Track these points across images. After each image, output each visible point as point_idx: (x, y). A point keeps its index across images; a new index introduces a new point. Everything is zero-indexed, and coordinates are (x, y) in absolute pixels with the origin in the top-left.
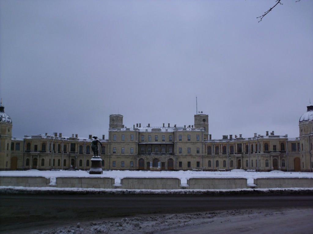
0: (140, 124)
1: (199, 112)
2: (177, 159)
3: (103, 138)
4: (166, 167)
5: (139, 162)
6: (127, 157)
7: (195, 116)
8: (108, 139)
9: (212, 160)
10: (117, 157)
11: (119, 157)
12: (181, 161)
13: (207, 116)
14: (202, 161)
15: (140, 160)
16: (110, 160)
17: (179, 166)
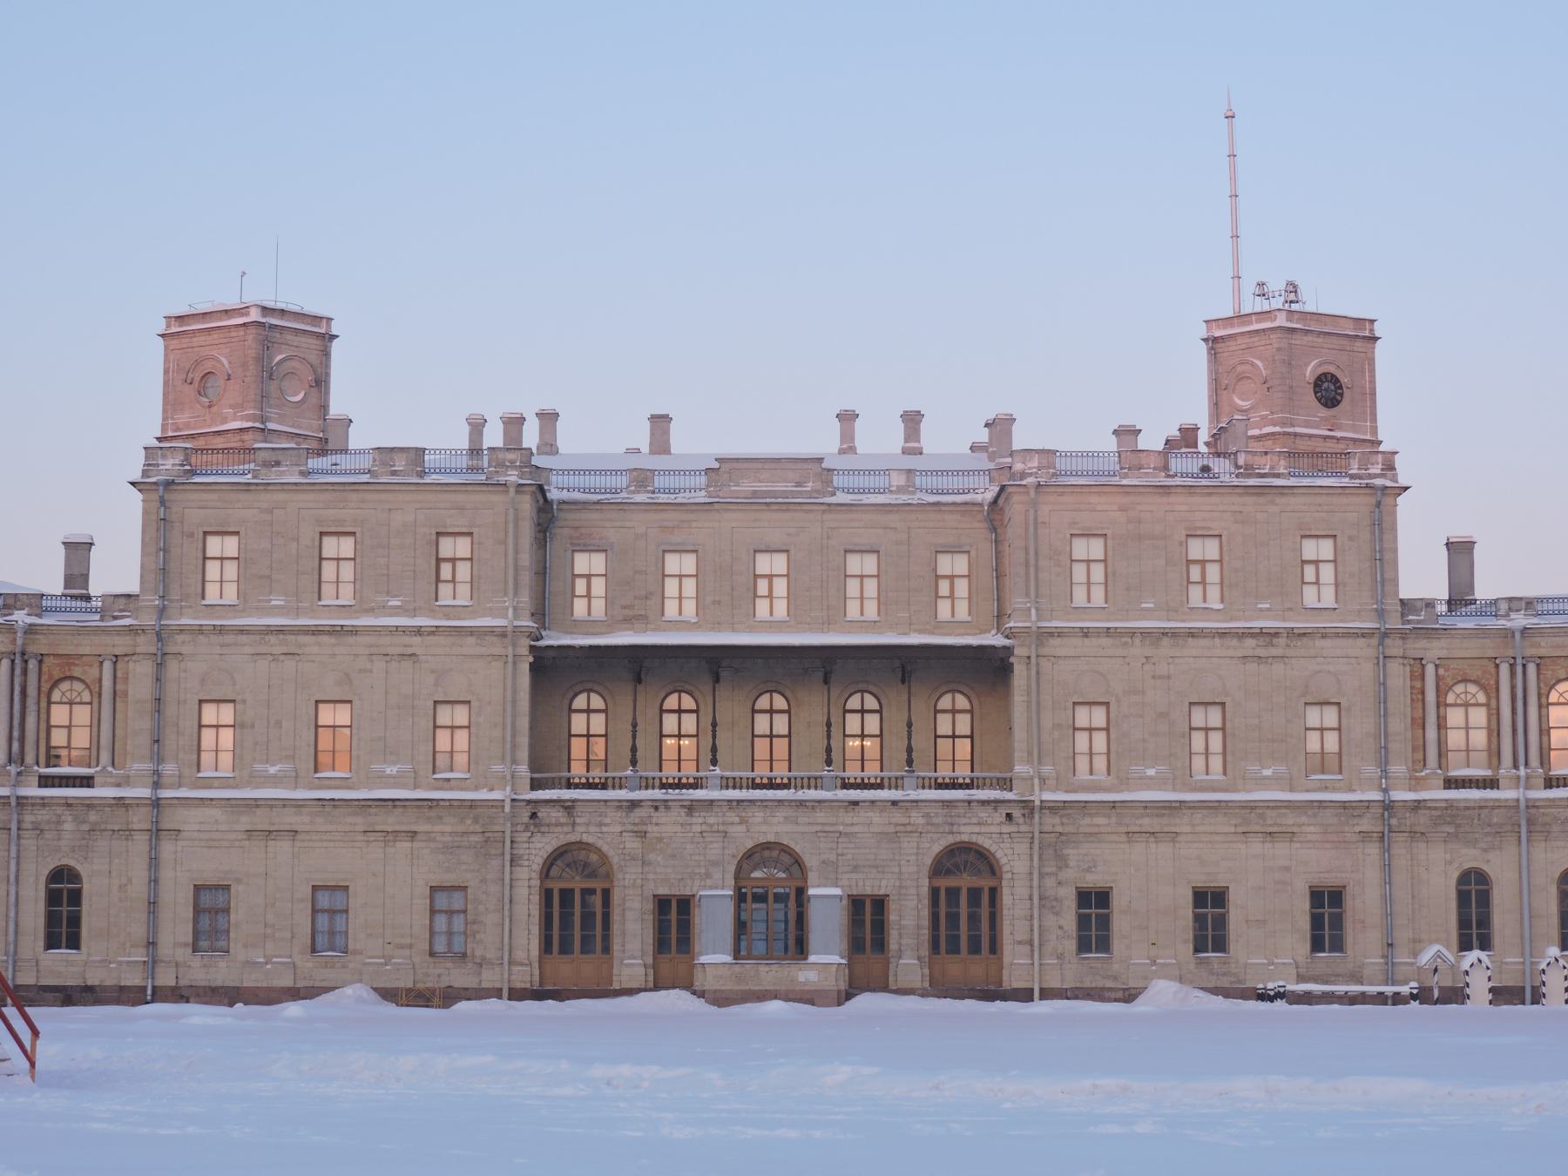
0: (548, 419)
1: (1262, 291)
2: (1052, 849)
3: (76, 578)
4: (908, 960)
5: (547, 895)
6: (391, 821)
7: (1213, 342)
8: (133, 587)
9: (1501, 868)
10: (245, 822)
11: (290, 819)
12: (1093, 880)
13: (1362, 335)
14: (1372, 875)
15: (546, 872)
16: (154, 862)
17: (1071, 945)
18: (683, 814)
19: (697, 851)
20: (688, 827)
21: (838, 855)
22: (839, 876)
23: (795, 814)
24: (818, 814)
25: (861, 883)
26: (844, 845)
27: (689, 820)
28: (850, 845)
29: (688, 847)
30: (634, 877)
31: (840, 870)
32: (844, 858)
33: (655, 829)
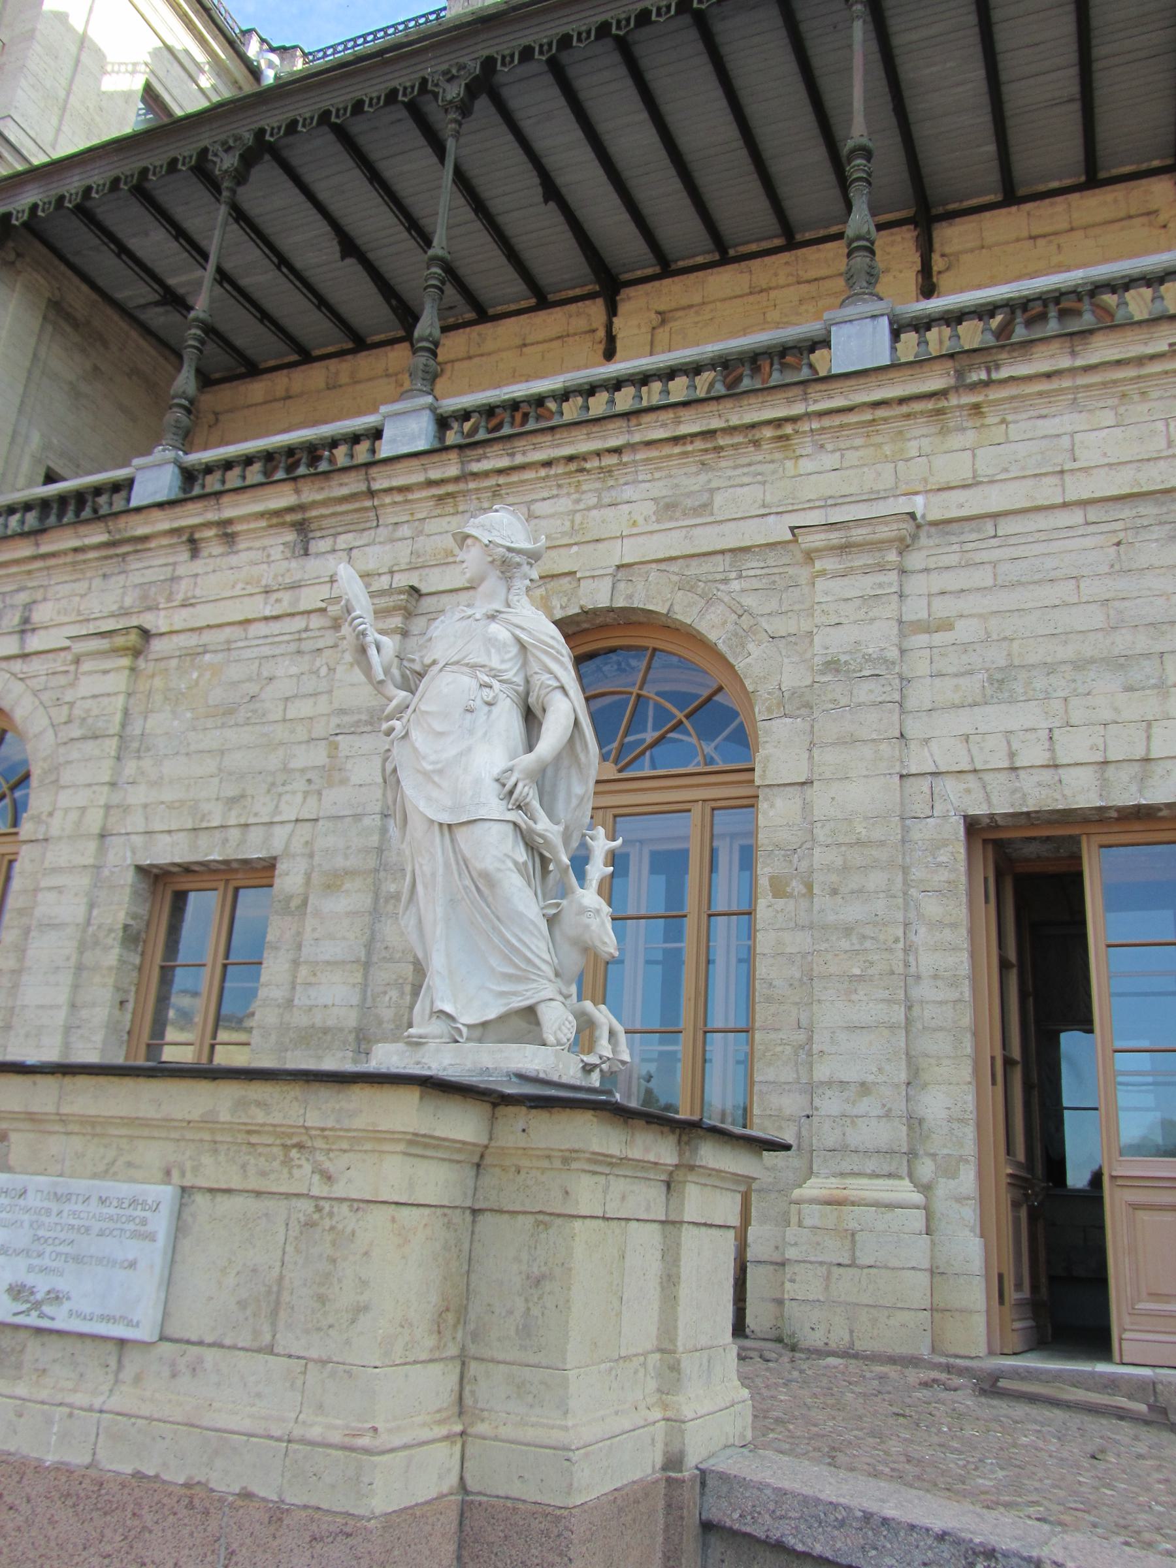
18: (277, 553)
19: (309, 684)
20: (286, 596)
21: (905, 627)
22: (914, 729)
23: (703, 478)
24: (806, 465)
25: (1033, 754)
26: (937, 582)
27: (297, 569)
28: (951, 581)
29: (280, 672)
30: (81, 798)
31: (919, 696)
32: (938, 638)
33: (182, 618)
